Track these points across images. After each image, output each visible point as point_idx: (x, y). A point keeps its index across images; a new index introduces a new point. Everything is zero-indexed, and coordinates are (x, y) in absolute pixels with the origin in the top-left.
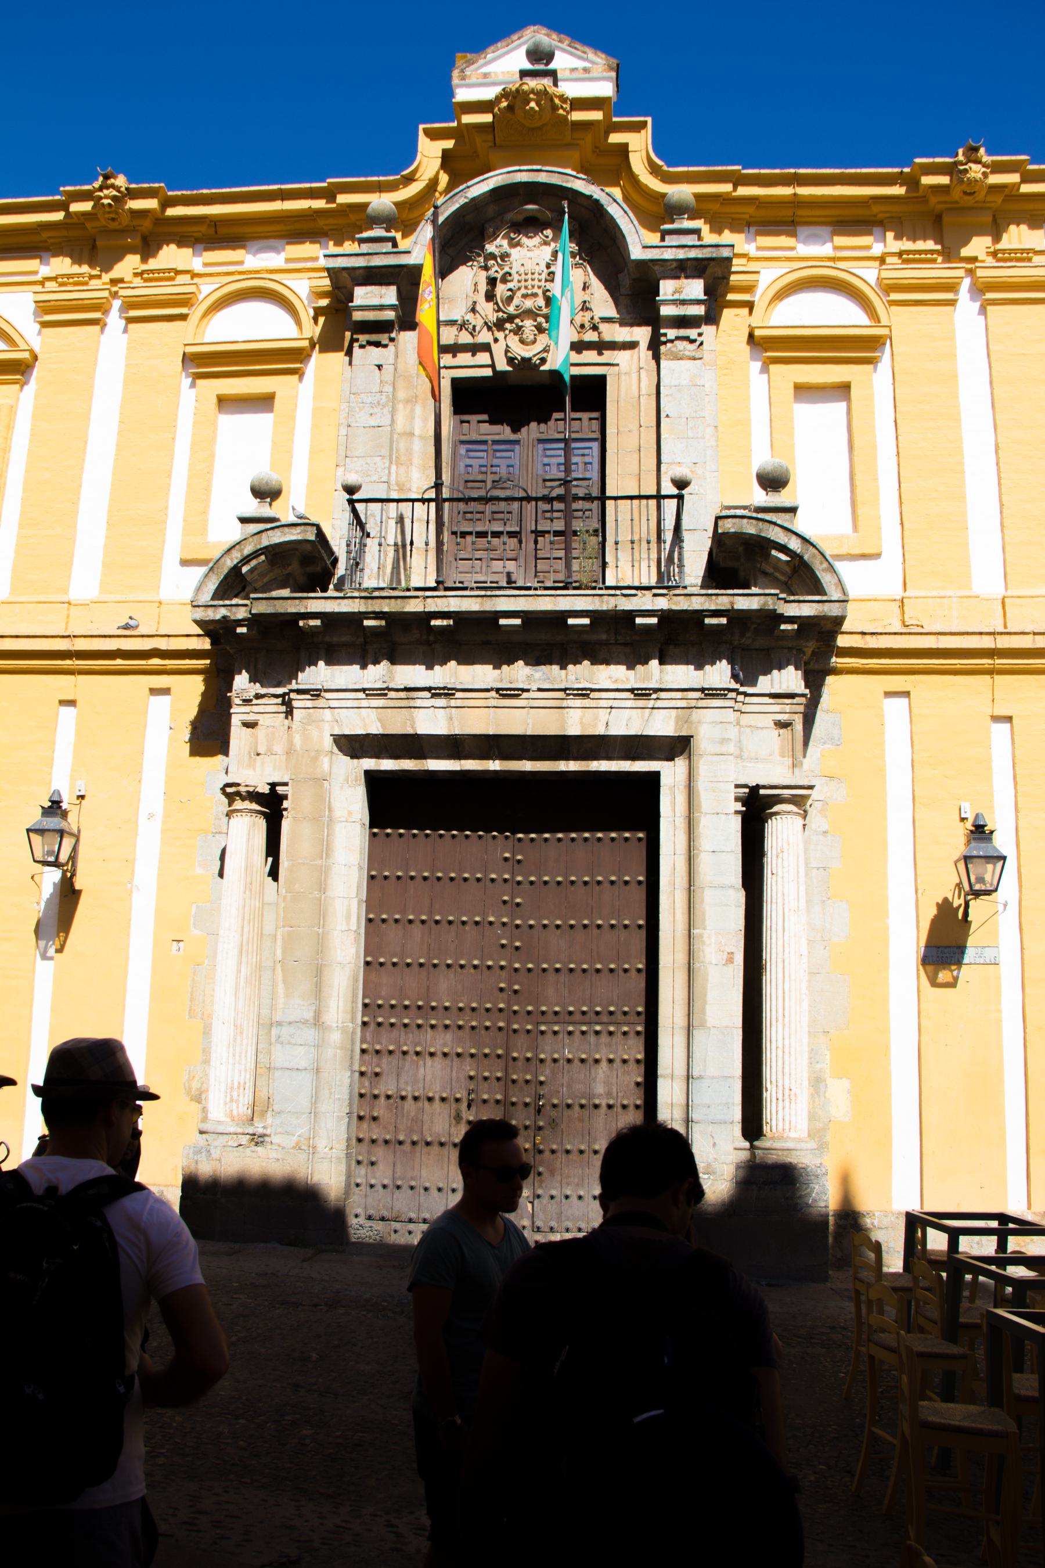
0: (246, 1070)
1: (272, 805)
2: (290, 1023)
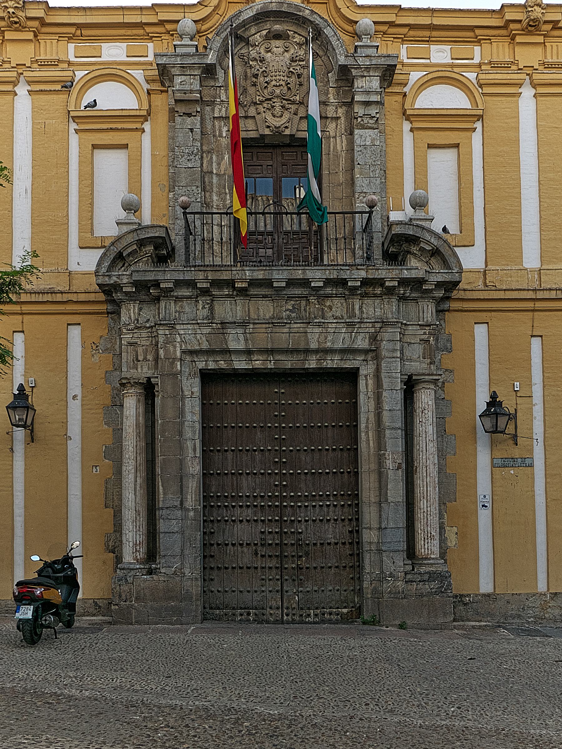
1: (148, 390)
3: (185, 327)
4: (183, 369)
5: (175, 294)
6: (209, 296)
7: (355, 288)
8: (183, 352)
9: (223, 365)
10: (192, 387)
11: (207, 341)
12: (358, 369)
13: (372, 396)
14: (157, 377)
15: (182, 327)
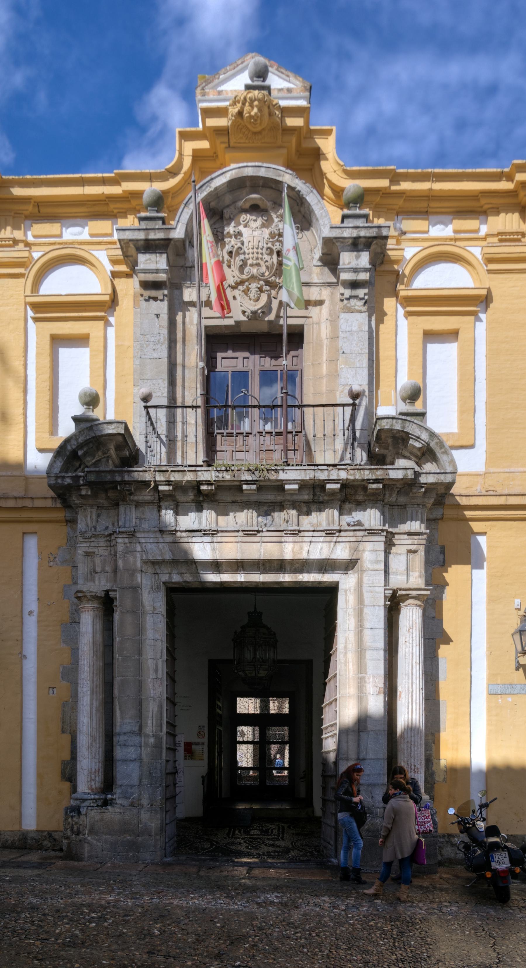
0: (99, 762)
1: (107, 604)
2: (125, 733)
3: (146, 535)
4: (144, 582)
5: (136, 498)
6: (173, 500)
7: (333, 493)
8: (145, 562)
9: (188, 578)
10: (154, 604)
11: (171, 551)
12: (337, 583)
13: (353, 613)
14: (115, 591)
15: (143, 535)
